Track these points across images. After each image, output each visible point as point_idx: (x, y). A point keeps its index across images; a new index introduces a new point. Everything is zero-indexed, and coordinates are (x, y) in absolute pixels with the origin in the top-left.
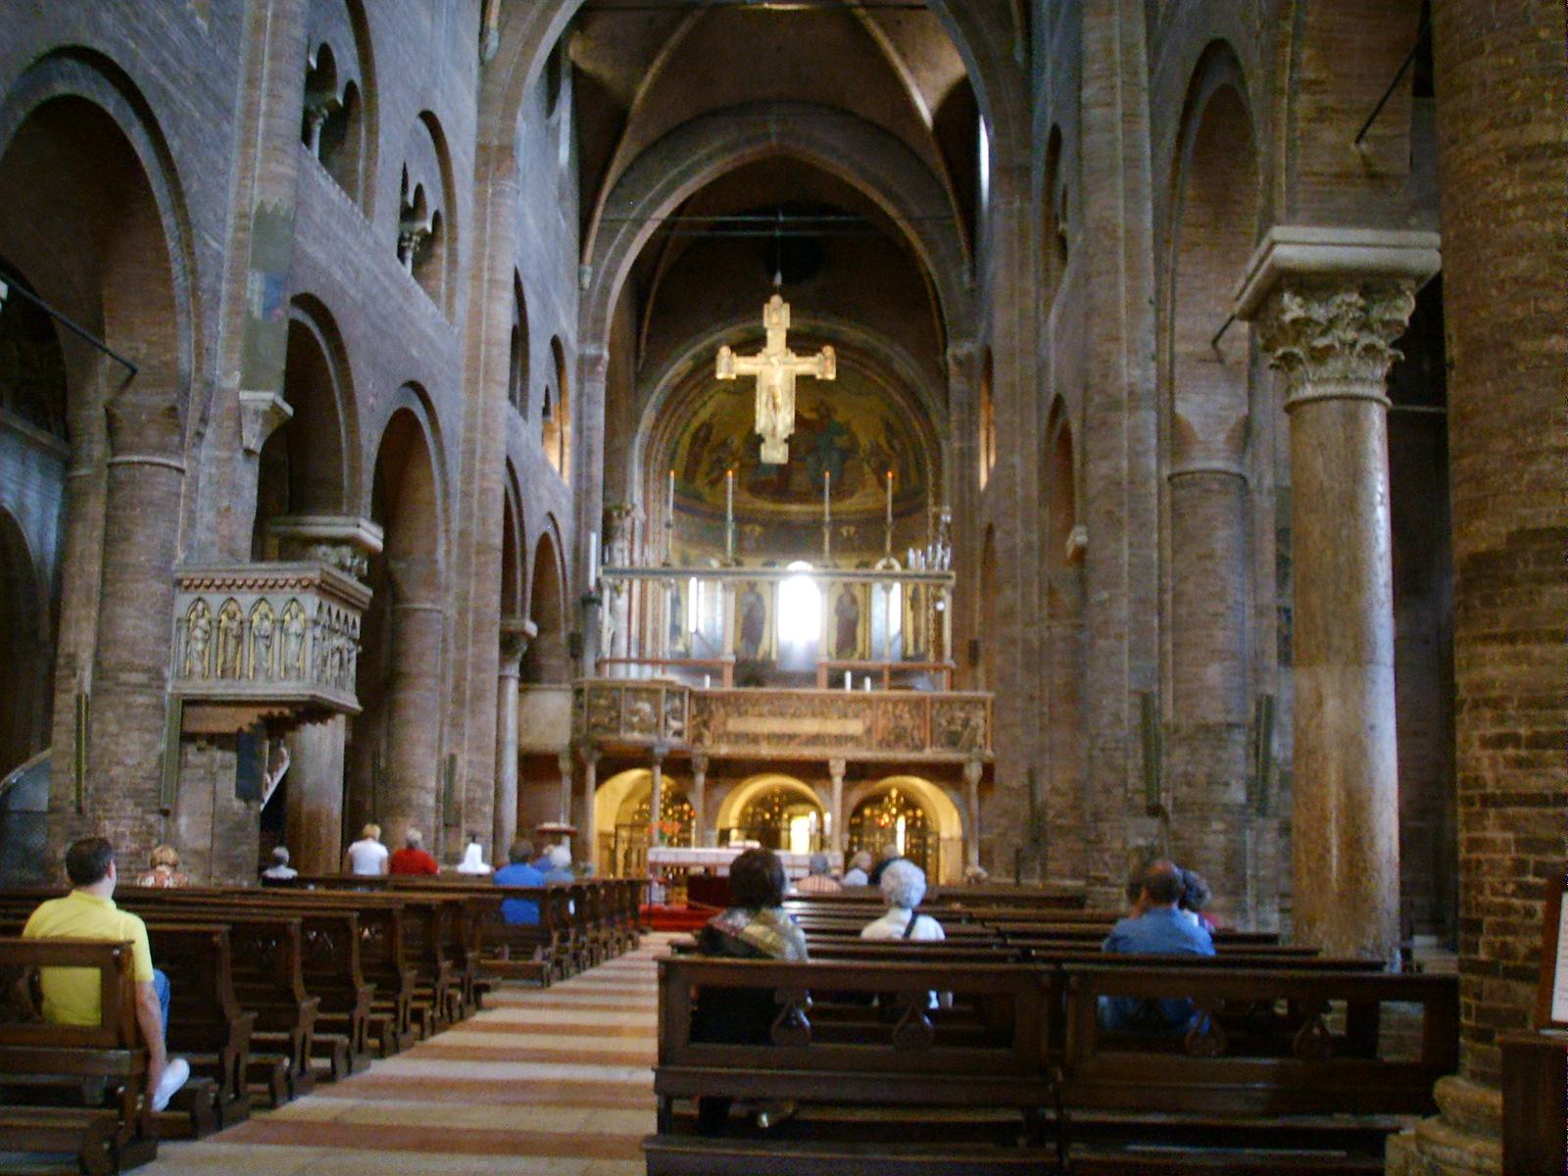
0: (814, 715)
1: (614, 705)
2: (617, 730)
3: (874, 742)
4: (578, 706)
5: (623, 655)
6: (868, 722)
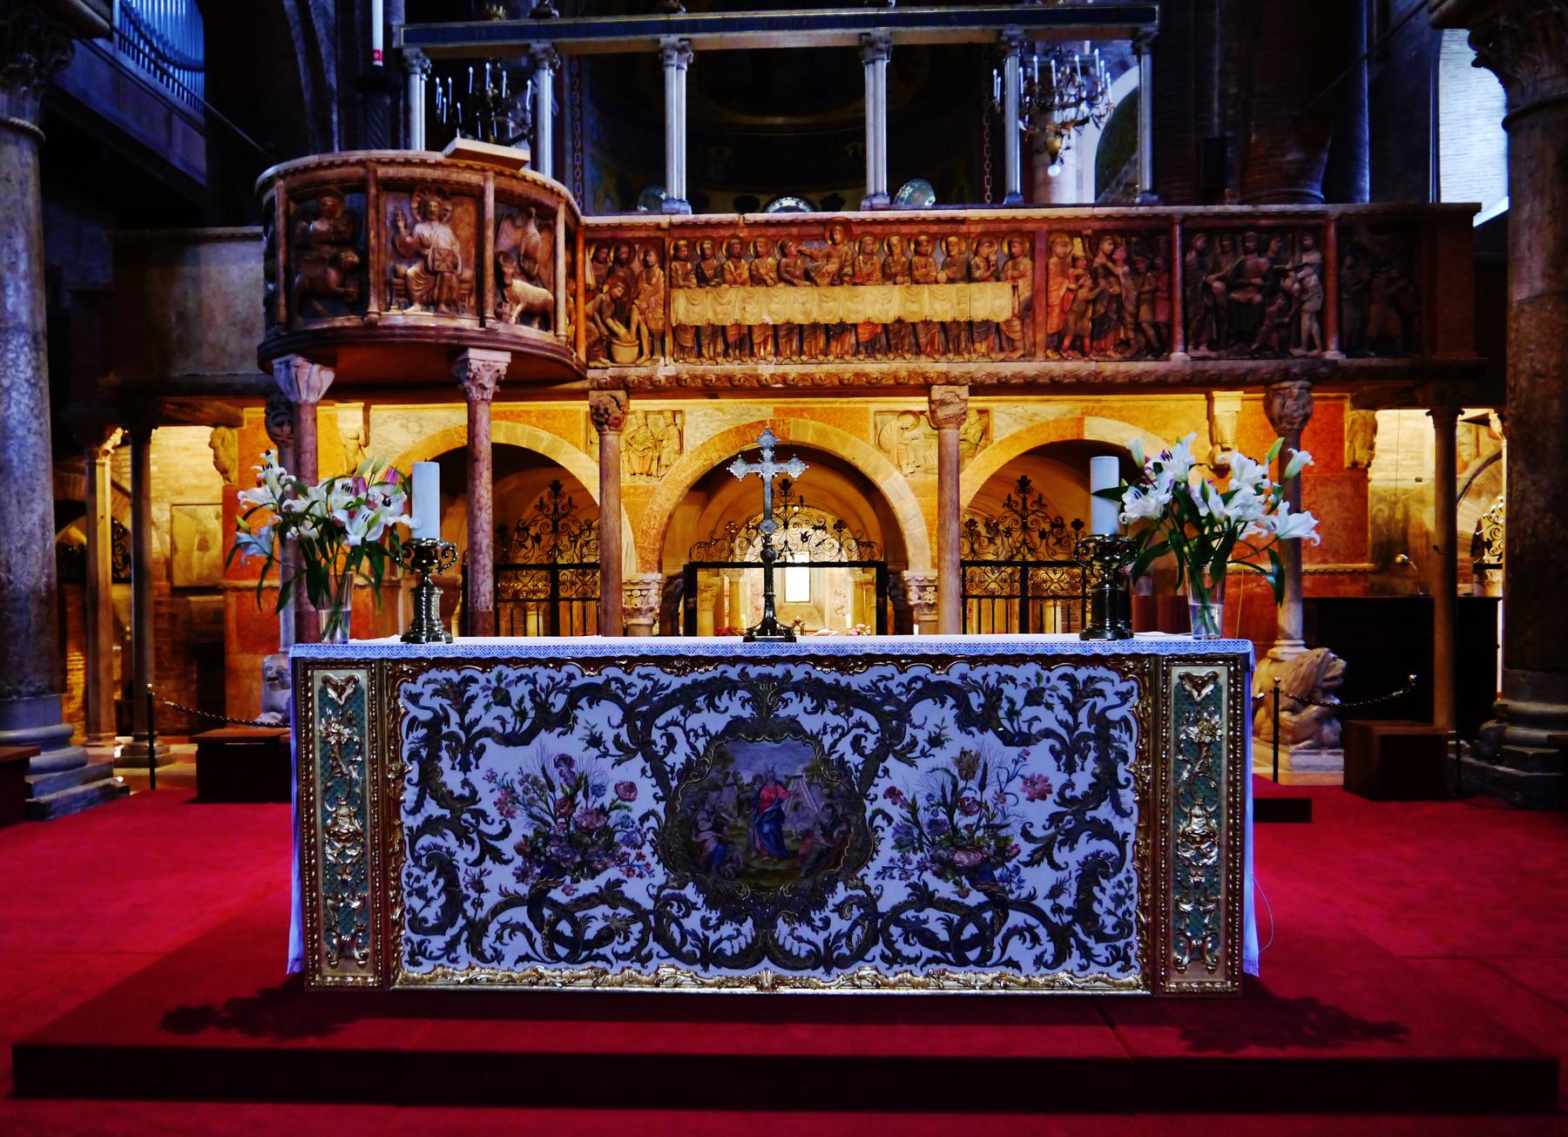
0: (888, 276)
1: (353, 233)
2: (360, 306)
3: (1040, 337)
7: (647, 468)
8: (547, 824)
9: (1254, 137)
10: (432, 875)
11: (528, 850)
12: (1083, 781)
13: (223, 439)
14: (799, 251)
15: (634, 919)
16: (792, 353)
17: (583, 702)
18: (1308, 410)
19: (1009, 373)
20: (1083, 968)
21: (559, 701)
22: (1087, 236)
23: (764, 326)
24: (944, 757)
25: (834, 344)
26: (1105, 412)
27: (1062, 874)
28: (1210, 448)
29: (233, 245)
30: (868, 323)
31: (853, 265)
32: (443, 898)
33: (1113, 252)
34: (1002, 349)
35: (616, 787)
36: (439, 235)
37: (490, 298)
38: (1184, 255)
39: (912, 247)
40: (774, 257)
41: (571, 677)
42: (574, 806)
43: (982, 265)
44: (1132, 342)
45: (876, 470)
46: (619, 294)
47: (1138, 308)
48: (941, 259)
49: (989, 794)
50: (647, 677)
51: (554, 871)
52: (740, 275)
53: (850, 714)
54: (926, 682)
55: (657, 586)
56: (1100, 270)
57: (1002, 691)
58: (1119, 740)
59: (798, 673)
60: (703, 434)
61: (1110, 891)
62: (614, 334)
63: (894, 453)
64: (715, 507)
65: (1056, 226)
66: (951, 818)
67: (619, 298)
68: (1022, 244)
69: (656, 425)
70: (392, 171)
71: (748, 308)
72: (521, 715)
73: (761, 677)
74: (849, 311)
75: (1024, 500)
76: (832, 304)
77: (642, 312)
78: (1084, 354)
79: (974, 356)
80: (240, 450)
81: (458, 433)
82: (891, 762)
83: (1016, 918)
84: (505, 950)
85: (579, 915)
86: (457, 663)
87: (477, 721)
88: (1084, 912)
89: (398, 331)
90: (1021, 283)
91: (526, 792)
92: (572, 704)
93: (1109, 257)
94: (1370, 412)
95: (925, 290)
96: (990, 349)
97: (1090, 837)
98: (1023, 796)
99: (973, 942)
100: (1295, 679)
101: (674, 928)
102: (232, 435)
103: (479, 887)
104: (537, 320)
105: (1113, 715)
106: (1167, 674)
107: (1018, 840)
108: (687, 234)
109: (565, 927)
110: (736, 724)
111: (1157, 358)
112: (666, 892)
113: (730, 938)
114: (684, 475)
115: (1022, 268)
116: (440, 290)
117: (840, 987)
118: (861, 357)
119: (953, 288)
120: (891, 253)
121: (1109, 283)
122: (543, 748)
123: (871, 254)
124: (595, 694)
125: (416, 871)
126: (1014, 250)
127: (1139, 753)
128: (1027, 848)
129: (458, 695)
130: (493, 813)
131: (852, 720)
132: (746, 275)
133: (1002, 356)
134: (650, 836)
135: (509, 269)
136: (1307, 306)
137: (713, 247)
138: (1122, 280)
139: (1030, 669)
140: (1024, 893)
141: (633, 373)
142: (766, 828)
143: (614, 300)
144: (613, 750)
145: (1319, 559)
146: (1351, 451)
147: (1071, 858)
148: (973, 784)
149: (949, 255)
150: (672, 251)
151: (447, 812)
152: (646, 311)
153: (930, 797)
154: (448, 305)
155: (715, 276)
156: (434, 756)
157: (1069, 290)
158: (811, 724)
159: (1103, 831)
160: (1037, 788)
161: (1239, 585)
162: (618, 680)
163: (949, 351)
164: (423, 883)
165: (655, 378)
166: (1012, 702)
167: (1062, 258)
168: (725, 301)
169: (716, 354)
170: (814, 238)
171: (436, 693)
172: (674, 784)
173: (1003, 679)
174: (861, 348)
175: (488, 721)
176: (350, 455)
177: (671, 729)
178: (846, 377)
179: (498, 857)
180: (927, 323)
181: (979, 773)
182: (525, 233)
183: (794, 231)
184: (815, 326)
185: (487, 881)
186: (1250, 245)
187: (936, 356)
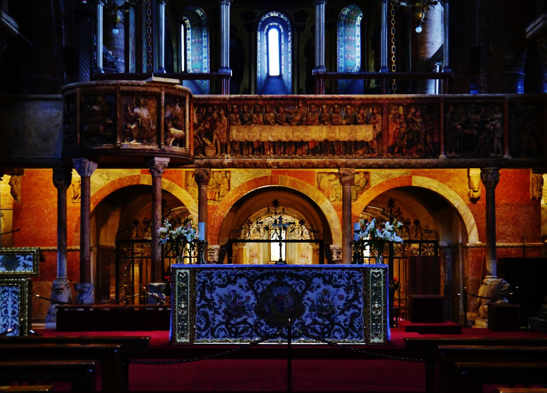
0: (321, 122)
2: (113, 140)
3: (385, 148)
4: (68, 116)
5: (122, 69)
6: (378, 127)
7: (213, 197)
8: (230, 305)
9: (491, 48)
10: (203, 317)
11: (225, 311)
12: (351, 296)
13: (16, 181)
14: (284, 111)
15: (249, 328)
16: (281, 153)
17: (238, 278)
18: (497, 179)
19: (371, 163)
20: (351, 339)
21: (233, 277)
22: (405, 106)
23: (269, 142)
24: (320, 290)
25: (298, 149)
26: (421, 174)
27: (347, 317)
28: (469, 190)
29: (40, 102)
30: (313, 141)
31: (307, 117)
32: (205, 323)
33: (415, 113)
34: (369, 153)
35: (246, 297)
36: (144, 113)
37: (163, 137)
38: (445, 114)
39: (332, 109)
40: (274, 113)
41: (236, 272)
42: (236, 302)
43: (361, 117)
44: (423, 151)
45: (318, 199)
46: (208, 127)
47: (426, 136)
48: (344, 115)
49: (330, 299)
50: (253, 272)
51: (231, 317)
52: (259, 120)
53: (299, 281)
54: (316, 273)
55: (217, 251)
56: (410, 120)
57: (333, 276)
58: (359, 287)
59: (287, 271)
60: (239, 182)
61: (357, 321)
62: (206, 144)
63: (326, 191)
64: (240, 212)
65: (392, 102)
66: (322, 304)
67: (207, 129)
68: (377, 109)
69: (218, 177)
70: (126, 88)
71: (263, 134)
72: (224, 281)
73: (279, 272)
74: (305, 136)
75: (391, 211)
76: (298, 133)
77: (217, 135)
78: (403, 155)
79: (357, 156)
80: (22, 186)
81: (125, 179)
82: (308, 292)
83: (336, 327)
84: (220, 335)
85: (237, 326)
86: (210, 269)
87: (214, 282)
88: (351, 325)
89: (128, 151)
90: (377, 125)
91: (225, 298)
92: (236, 278)
93: (414, 114)
94: (540, 175)
95: (337, 128)
96: (364, 153)
97: (353, 309)
98: (338, 299)
99: (327, 332)
100: (489, 291)
101: (259, 330)
102: (19, 178)
103: (214, 320)
104: (178, 143)
105: (358, 281)
106: (369, 272)
107: (336, 309)
108: (237, 103)
109: (234, 329)
110: (273, 283)
111: (433, 158)
112: (257, 321)
113: (271, 332)
114: (230, 200)
115: (377, 119)
116: (144, 133)
117: (296, 342)
118: (310, 155)
119: (348, 127)
120: (323, 112)
121: (414, 126)
122: (229, 288)
123: (315, 112)
124: (241, 276)
125: (199, 317)
126: (374, 111)
127: (364, 289)
128: (339, 311)
129: (210, 276)
130: (217, 303)
131: (299, 282)
132: (262, 120)
133: (369, 156)
134: (253, 308)
135: (169, 125)
136: (497, 136)
137: (248, 108)
138: (419, 124)
139: (339, 271)
140: (338, 321)
141: (214, 161)
142: (280, 306)
143: (206, 129)
144: (245, 289)
145: (519, 241)
146: (533, 192)
147: (349, 313)
148: (326, 296)
149: (347, 113)
150: (230, 110)
151: (206, 303)
152: (219, 135)
153: (317, 299)
154: (146, 140)
155: (249, 120)
156: (204, 290)
157: (397, 128)
158: (290, 283)
159: (356, 307)
160: (341, 298)
161: (482, 252)
162: (246, 273)
163: (347, 153)
164: (201, 319)
165: (223, 164)
166: (335, 278)
167: (394, 115)
168: (253, 131)
169: (249, 154)
170: (290, 105)
171: (204, 276)
172: (259, 296)
173: (333, 273)
174: (310, 152)
175: (216, 282)
176: (76, 189)
177: (259, 284)
178: (303, 164)
179: (219, 313)
180: (338, 141)
181: (328, 294)
182: (175, 109)
183: (282, 102)
184: (291, 142)
185: (216, 319)
186: (472, 110)
187: (342, 156)
